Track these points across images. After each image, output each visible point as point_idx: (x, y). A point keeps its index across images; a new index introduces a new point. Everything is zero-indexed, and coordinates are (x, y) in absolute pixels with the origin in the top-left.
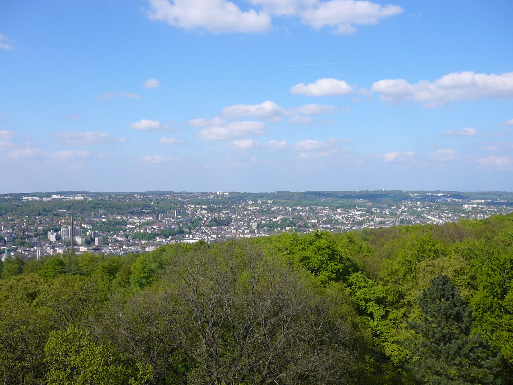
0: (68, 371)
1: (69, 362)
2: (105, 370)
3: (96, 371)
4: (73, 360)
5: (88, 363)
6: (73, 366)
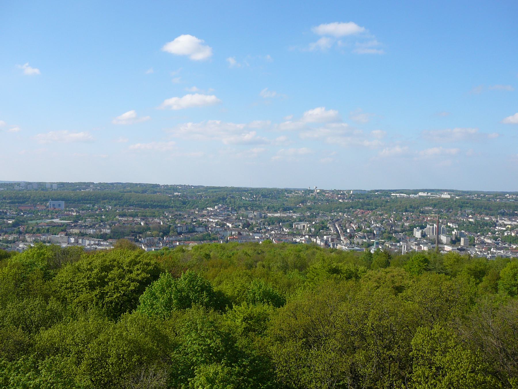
0: (434, 369)
1: (435, 361)
2: (472, 377)
3: (462, 376)
4: (438, 359)
5: (454, 365)
6: (438, 366)
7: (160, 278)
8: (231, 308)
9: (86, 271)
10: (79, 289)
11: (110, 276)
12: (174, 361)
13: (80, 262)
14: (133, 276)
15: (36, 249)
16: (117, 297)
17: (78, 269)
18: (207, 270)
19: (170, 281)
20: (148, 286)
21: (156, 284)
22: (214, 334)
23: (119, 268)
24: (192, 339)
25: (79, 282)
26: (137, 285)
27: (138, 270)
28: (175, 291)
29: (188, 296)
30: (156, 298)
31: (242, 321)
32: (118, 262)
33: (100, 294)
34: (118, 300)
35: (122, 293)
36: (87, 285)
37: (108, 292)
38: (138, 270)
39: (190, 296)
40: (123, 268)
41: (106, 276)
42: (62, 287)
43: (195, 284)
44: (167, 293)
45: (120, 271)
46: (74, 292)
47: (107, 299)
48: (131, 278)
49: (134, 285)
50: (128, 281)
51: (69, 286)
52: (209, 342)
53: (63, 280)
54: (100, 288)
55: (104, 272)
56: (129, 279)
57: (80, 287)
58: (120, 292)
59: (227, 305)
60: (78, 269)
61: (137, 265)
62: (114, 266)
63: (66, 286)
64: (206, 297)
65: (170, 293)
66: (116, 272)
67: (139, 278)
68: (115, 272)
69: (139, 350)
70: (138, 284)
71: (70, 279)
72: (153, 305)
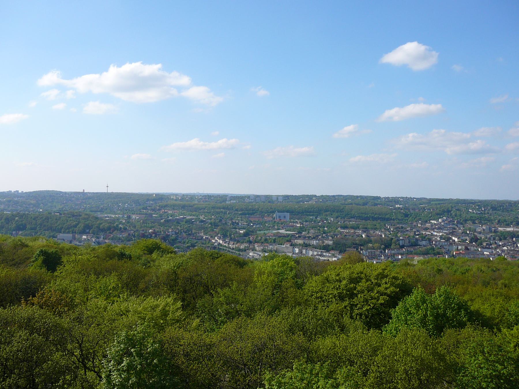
7: (413, 293)
8: (500, 330)
9: (335, 282)
10: (328, 299)
11: (359, 288)
12: (460, 383)
13: (328, 272)
14: (382, 289)
15: (280, 259)
16: (367, 310)
17: (327, 279)
18: (453, 287)
19: (424, 296)
20: (401, 300)
21: (411, 299)
22: (505, 360)
23: (367, 281)
24: (479, 362)
25: (328, 292)
26: (386, 298)
27: (386, 283)
28: (431, 307)
29: (444, 315)
30: (410, 313)
31: (515, 346)
32: (365, 275)
33: (350, 306)
34: (368, 313)
35: (372, 306)
36: (336, 296)
37: (357, 304)
38: (386, 283)
39: (447, 314)
40: (371, 281)
41: (355, 288)
42: (313, 296)
43: (451, 301)
44: (422, 310)
45: (368, 283)
46: (324, 301)
47: (356, 311)
48: (380, 291)
49: (384, 298)
50: (378, 294)
51: (319, 295)
52: (500, 367)
53: (313, 290)
54: (350, 299)
55: (353, 284)
56: (378, 292)
57: (330, 297)
58: (370, 305)
59: (495, 327)
60: (327, 279)
61: (385, 279)
62: (362, 279)
63: (317, 295)
64: (465, 316)
65: (425, 309)
66: (365, 284)
67: (388, 291)
68: (363, 285)
69: (430, 368)
70: (388, 298)
71: (320, 289)
72: (406, 320)
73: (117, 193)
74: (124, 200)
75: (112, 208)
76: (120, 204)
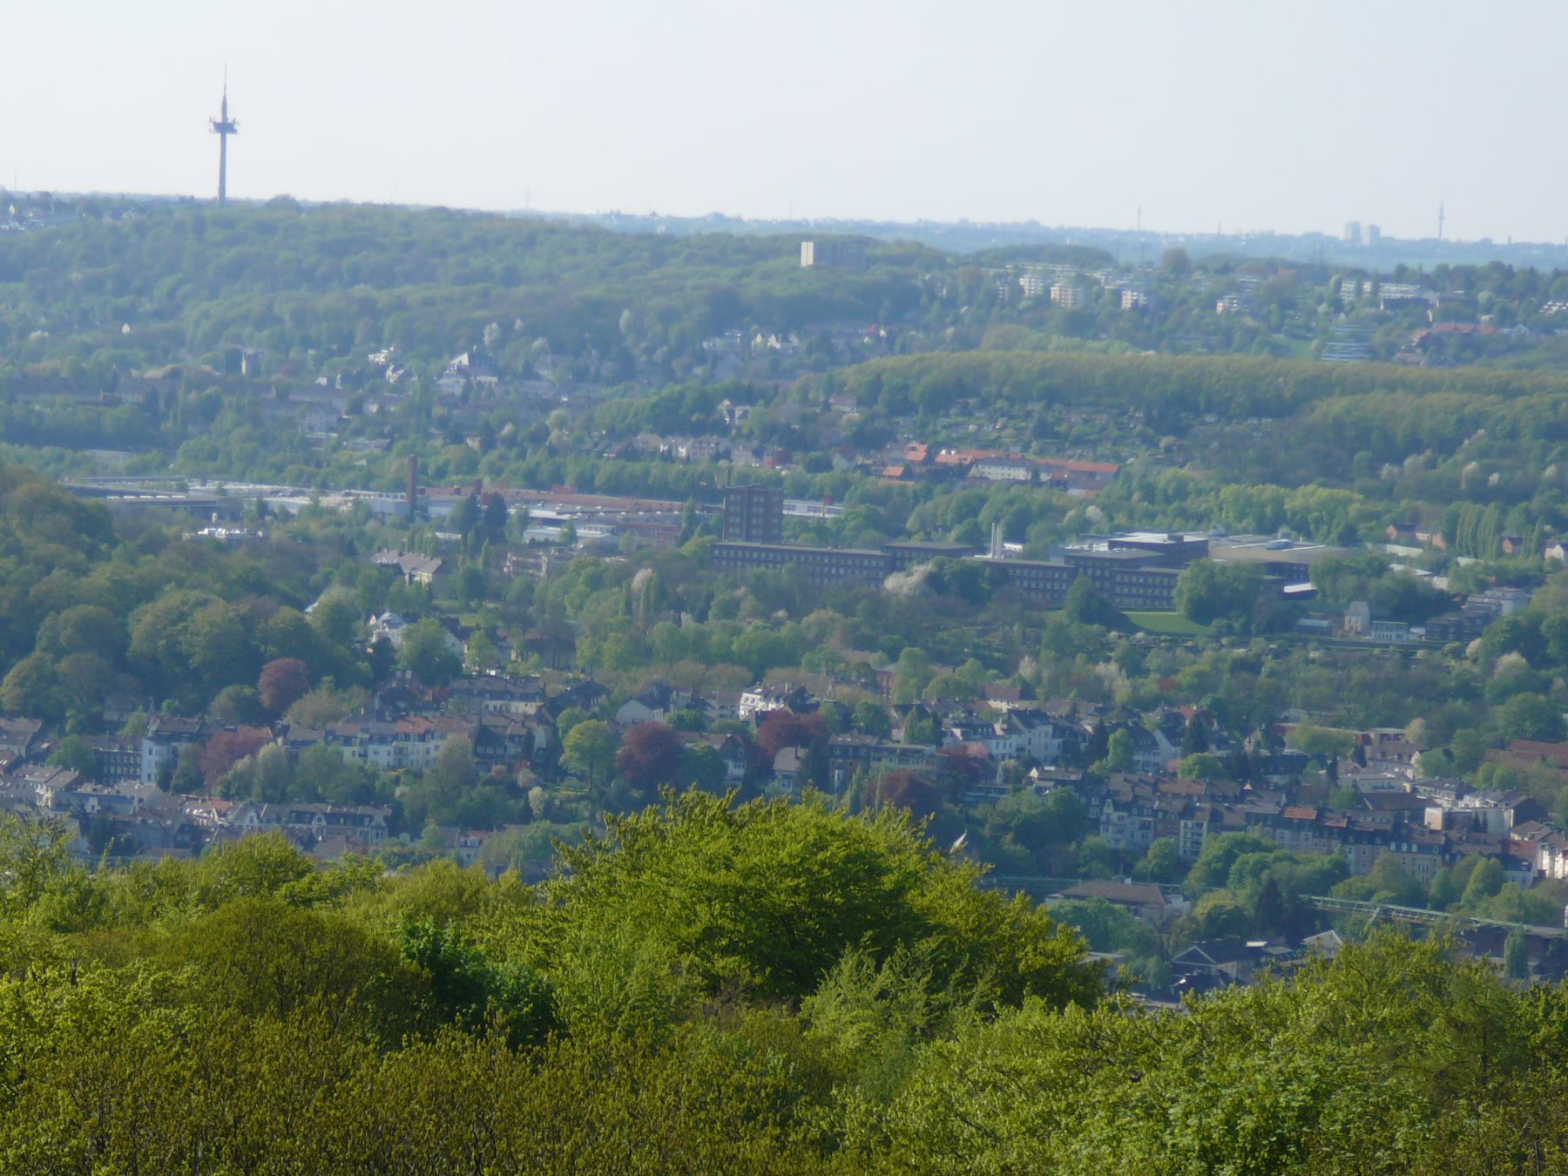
73: (345, 207)
74: (428, 303)
75: (283, 397)
76: (380, 358)
